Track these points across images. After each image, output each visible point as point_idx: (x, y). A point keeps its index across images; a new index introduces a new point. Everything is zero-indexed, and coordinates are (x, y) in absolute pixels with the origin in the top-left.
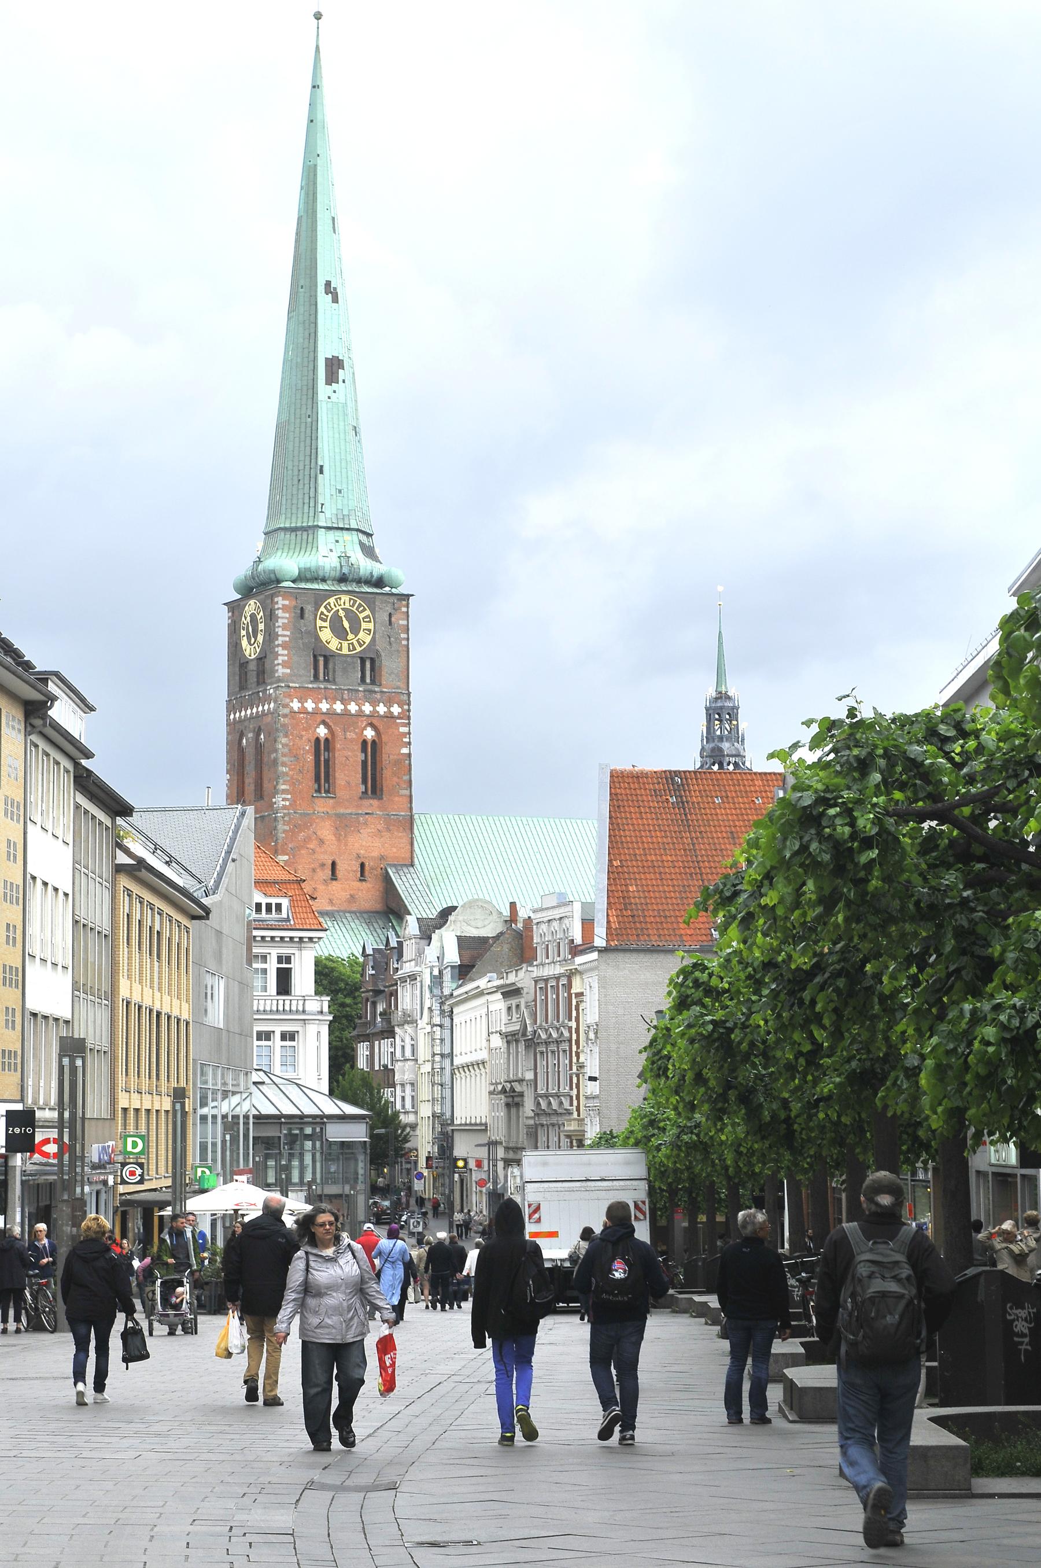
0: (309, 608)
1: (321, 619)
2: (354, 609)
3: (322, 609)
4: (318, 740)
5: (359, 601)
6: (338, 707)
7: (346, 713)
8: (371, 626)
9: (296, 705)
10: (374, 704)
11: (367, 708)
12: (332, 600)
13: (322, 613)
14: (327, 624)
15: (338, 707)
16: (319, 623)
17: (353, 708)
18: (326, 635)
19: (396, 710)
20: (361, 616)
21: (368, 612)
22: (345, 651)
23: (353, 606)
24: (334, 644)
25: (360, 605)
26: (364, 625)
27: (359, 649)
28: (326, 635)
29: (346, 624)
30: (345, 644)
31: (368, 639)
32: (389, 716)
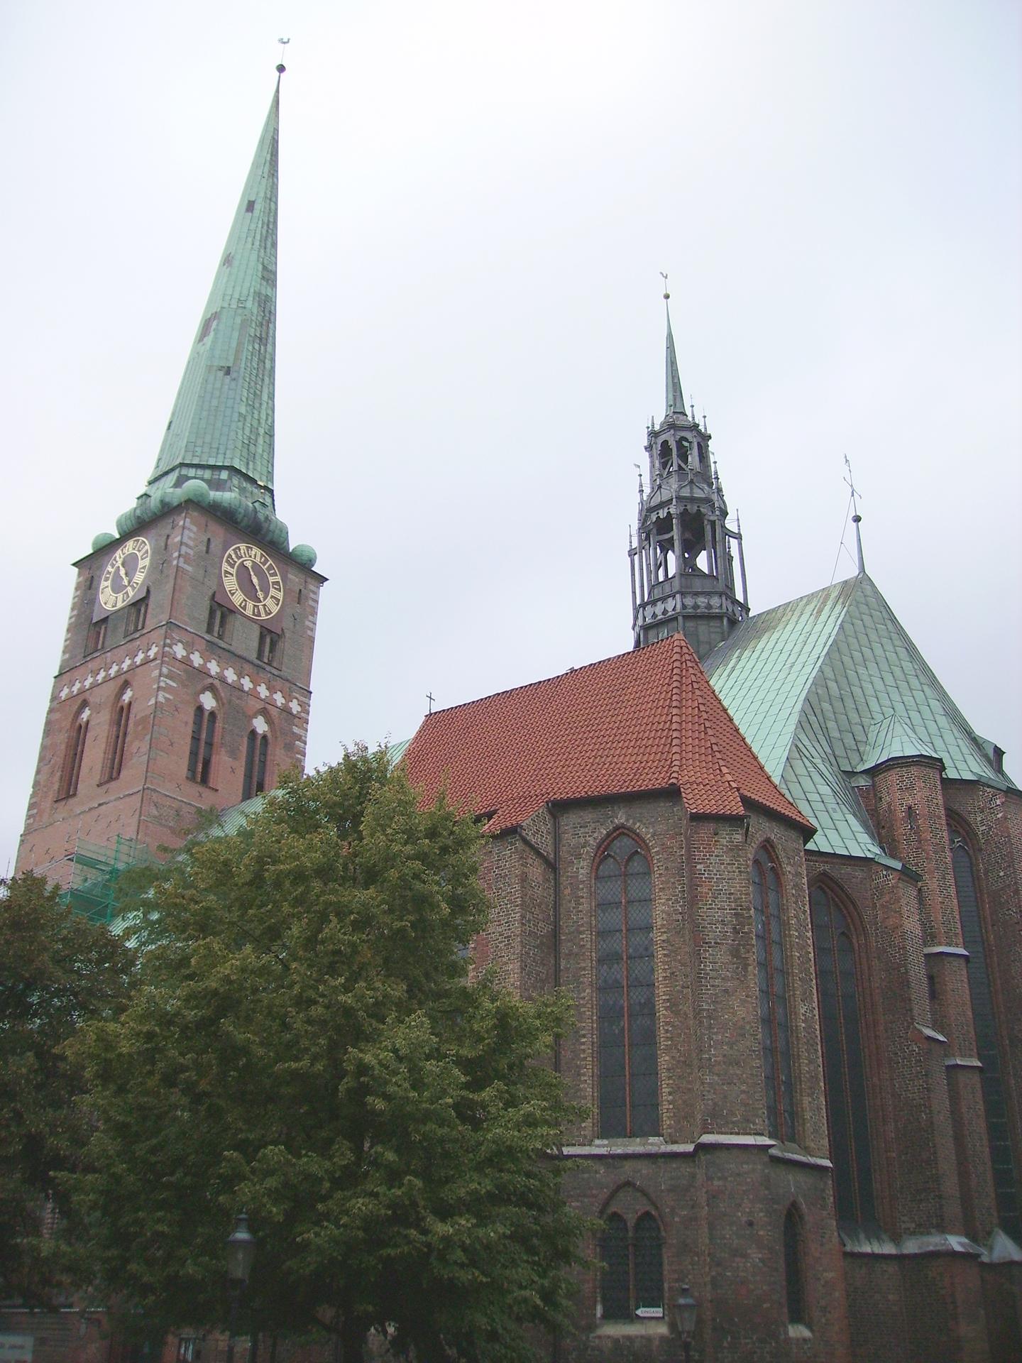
0: (216, 545)
1: (227, 561)
2: (265, 568)
3: (230, 551)
4: (200, 709)
5: (270, 562)
6: (231, 676)
8: (280, 595)
9: (180, 651)
12: (243, 546)
13: (230, 556)
14: (233, 571)
15: (231, 676)
16: (225, 566)
18: (230, 583)
19: (295, 707)
20: (271, 579)
22: (249, 612)
24: (238, 598)
25: (271, 567)
26: (272, 592)
27: (264, 617)
28: (230, 583)
29: (255, 580)
30: (250, 605)
31: (275, 610)
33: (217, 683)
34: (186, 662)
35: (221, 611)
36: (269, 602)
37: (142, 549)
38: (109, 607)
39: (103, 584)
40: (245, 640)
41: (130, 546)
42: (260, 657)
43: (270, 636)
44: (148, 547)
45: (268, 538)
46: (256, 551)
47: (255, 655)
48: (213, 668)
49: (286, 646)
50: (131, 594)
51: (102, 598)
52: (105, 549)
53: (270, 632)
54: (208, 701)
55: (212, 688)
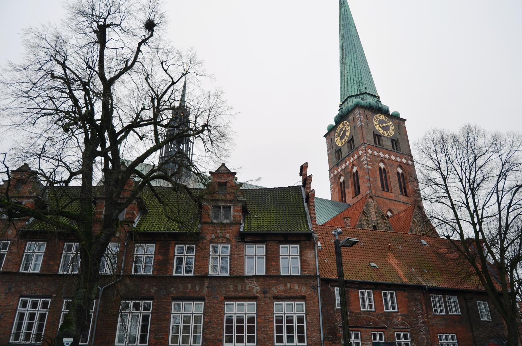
3: (375, 118)
6: (387, 156)
7: (390, 159)
8: (393, 128)
9: (370, 151)
10: (401, 159)
11: (399, 160)
12: (378, 115)
15: (387, 156)
16: (374, 123)
17: (393, 158)
18: (377, 127)
21: (391, 123)
22: (386, 135)
23: (386, 119)
24: (381, 132)
26: (391, 127)
27: (390, 136)
30: (385, 132)
31: (393, 133)
32: (407, 164)
33: (384, 159)
34: (372, 155)
35: (377, 137)
36: (391, 130)
37: (345, 125)
38: (340, 145)
39: (336, 139)
40: (388, 144)
41: (341, 125)
42: (393, 148)
43: (395, 142)
44: (348, 123)
45: (383, 111)
46: (382, 116)
47: (392, 147)
48: (381, 154)
49: (401, 143)
50: (347, 139)
51: (337, 143)
52: (332, 130)
53: (394, 140)
54: (382, 165)
55: (382, 161)
